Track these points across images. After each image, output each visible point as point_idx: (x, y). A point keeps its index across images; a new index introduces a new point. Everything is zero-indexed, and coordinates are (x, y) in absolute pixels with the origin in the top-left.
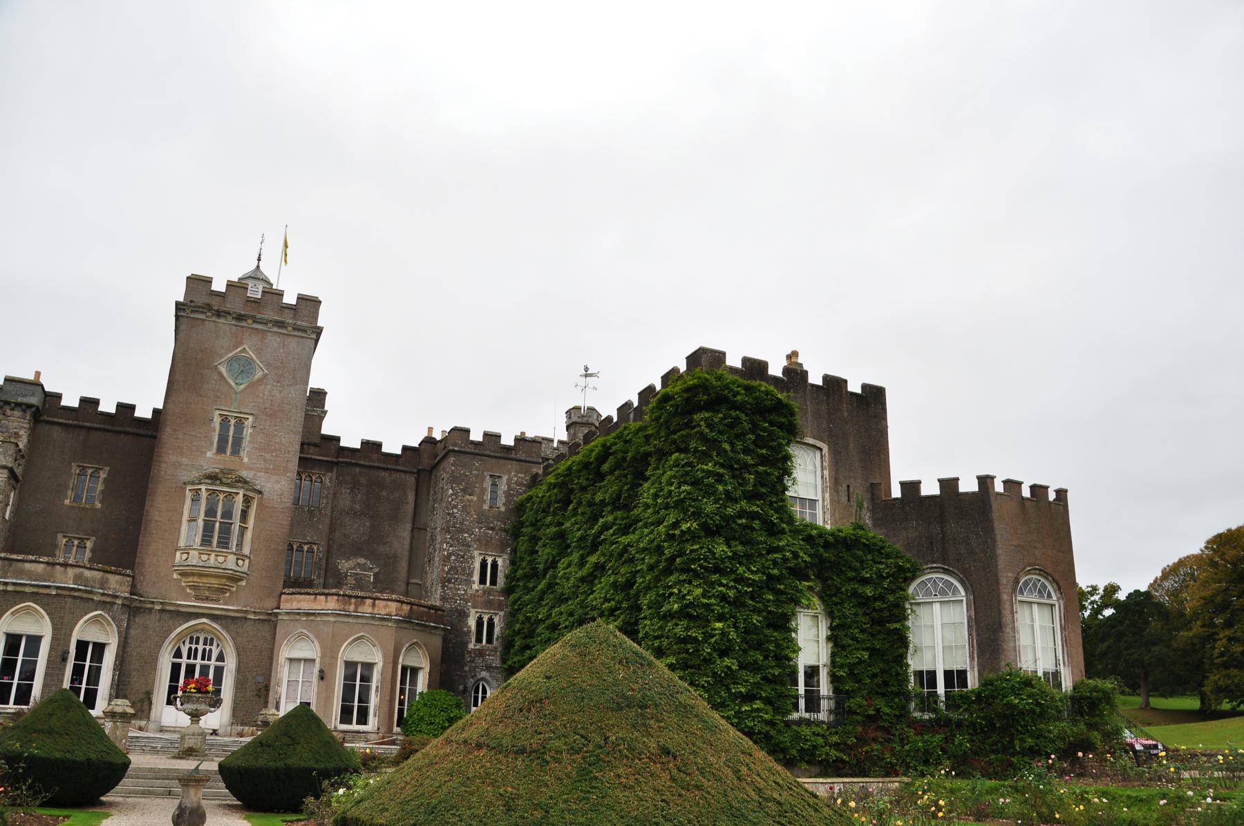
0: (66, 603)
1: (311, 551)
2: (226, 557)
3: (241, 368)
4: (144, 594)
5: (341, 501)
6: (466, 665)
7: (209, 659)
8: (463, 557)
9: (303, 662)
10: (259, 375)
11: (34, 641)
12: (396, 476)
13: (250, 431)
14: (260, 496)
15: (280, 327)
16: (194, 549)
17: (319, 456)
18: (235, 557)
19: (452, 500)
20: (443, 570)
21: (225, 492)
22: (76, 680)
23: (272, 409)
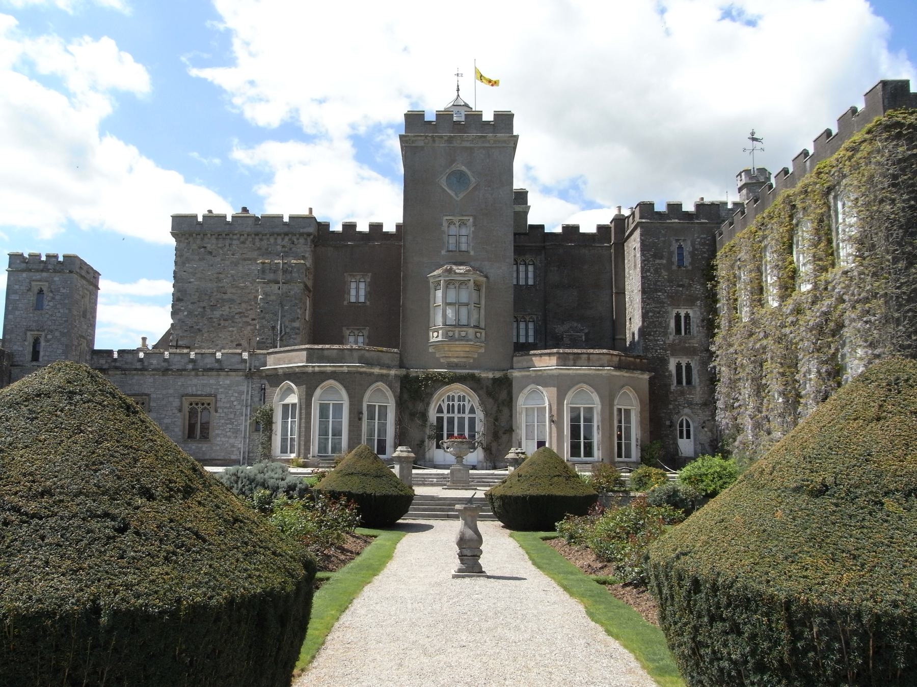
6: (671, 404)
7: (464, 412)
8: (659, 313)
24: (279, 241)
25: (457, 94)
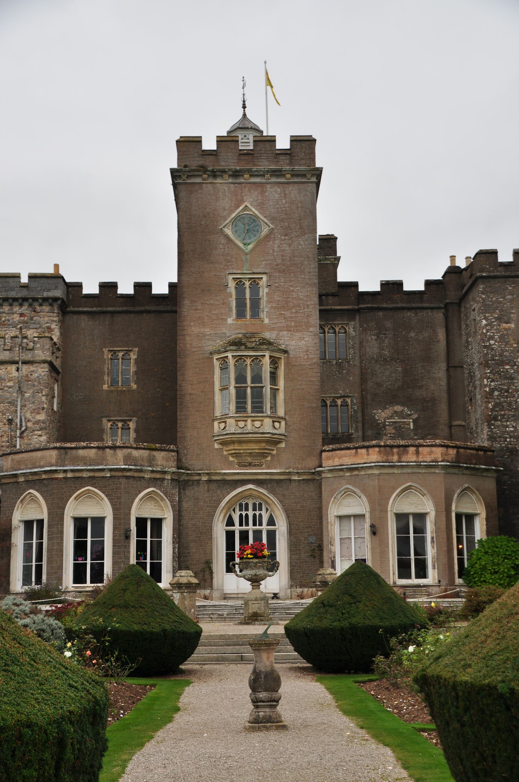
0: (121, 484)
1: (345, 404)
2: (262, 421)
3: (247, 227)
4: (190, 467)
5: (368, 349)
7: (261, 524)
9: (352, 519)
10: (265, 231)
11: (98, 522)
12: (421, 314)
13: (266, 290)
14: (286, 355)
15: (278, 176)
16: (231, 417)
17: (340, 305)
18: (271, 420)
19: (488, 331)
20: (487, 408)
21: (251, 356)
22: (140, 555)
23: (284, 265)
24: (16, 309)
25: (242, 114)
